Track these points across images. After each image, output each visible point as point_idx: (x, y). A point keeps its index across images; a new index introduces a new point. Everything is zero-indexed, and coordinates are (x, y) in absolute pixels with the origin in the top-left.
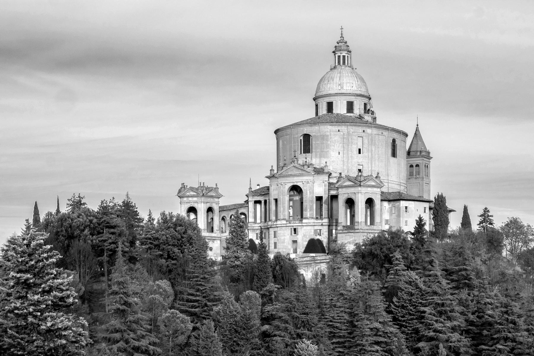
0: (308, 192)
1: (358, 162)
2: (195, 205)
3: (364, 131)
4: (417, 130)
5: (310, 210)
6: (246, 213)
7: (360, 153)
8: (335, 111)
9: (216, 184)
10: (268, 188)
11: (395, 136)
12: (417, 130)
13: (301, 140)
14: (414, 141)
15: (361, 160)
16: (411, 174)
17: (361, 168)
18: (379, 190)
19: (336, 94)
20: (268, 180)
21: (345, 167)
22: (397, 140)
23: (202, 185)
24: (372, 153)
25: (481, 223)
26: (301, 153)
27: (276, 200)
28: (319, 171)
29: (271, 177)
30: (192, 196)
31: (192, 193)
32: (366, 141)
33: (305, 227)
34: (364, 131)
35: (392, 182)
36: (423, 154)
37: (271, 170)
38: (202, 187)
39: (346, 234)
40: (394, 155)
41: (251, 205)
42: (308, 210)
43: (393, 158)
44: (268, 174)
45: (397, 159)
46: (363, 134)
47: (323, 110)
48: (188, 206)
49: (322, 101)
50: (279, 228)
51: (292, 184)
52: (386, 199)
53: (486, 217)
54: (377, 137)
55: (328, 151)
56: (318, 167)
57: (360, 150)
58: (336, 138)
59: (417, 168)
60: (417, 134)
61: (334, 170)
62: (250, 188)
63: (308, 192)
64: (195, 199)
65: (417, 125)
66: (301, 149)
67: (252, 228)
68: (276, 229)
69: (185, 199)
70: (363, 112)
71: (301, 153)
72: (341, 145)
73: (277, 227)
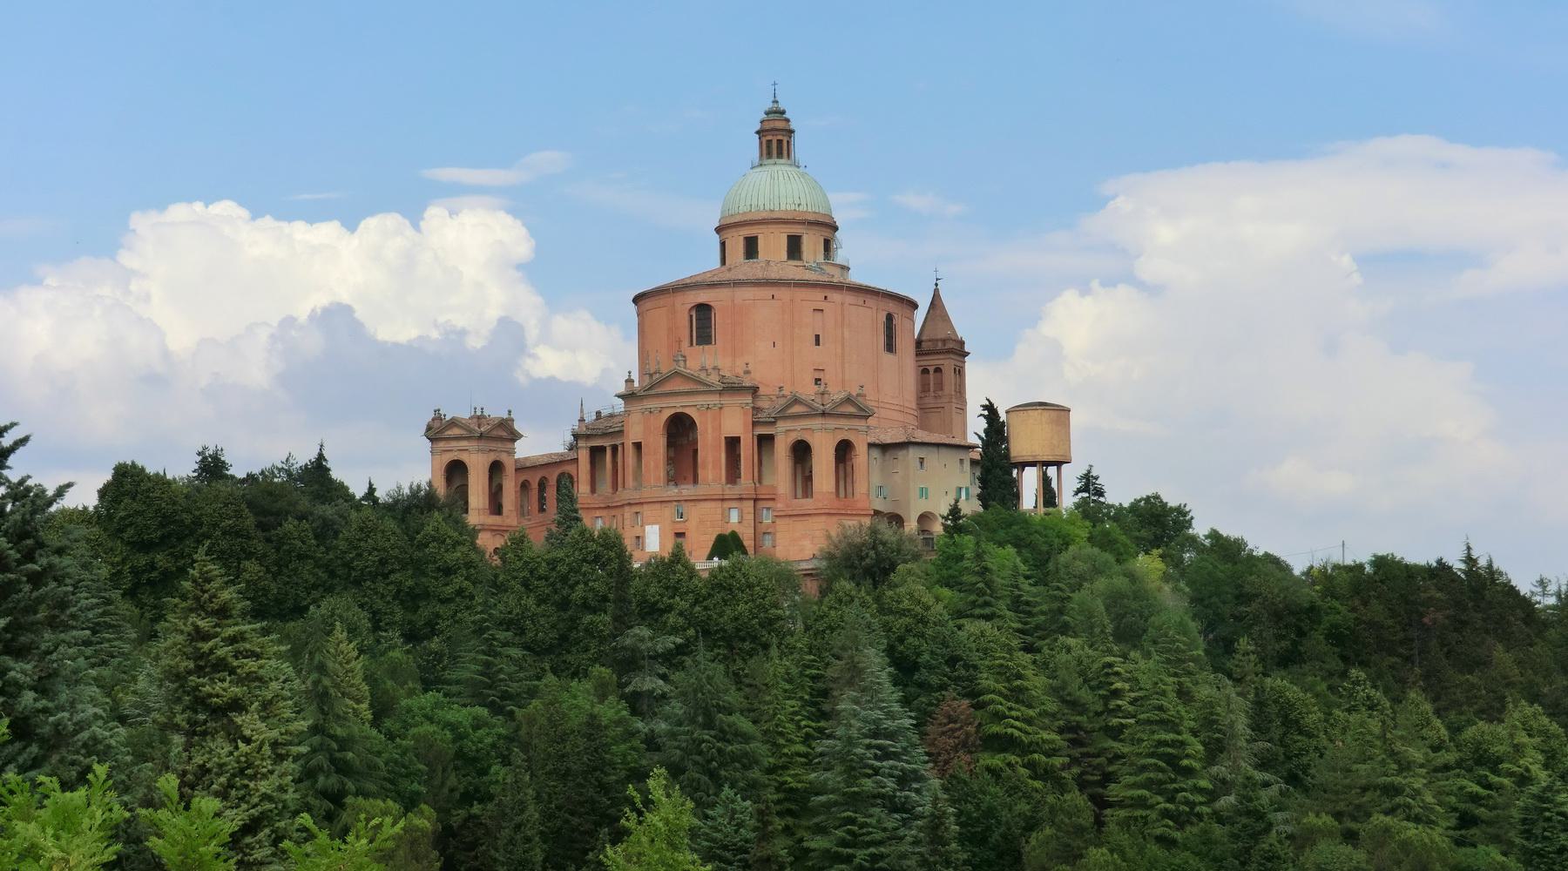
0: (709, 426)
2: (464, 457)
3: (826, 297)
6: (574, 473)
7: (818, 343)
9: (510, 412)
11: (892, 307)
13: (691, 316)
14: (929, 319)
16: (923, 389)
18: (863, 422)
20: (621, 401)
23: (479, 413)
24: (843, 345)
26: (692, 344)
27: (638, 446)
29: (628, 397)
35: (888, 406)
36: (950, 345)
37: (626, 381)
38: (479, 418)
40: (890, 347)
41: (584, 456)
42: (710, 466)
43: (890, 356)
44: (622, 389)
49: (735, 234)
50: (645, 506)
51: (673, 411)
52: (877, 442)
56: (728, 374)
57: (817, 337)
59: (938, 374)
60: (936, 303)
63: (709, 426)
64: (464, 444)
66: (691, 336)
70: (821, 259)
71: (692, 344)
73: (642, 503)
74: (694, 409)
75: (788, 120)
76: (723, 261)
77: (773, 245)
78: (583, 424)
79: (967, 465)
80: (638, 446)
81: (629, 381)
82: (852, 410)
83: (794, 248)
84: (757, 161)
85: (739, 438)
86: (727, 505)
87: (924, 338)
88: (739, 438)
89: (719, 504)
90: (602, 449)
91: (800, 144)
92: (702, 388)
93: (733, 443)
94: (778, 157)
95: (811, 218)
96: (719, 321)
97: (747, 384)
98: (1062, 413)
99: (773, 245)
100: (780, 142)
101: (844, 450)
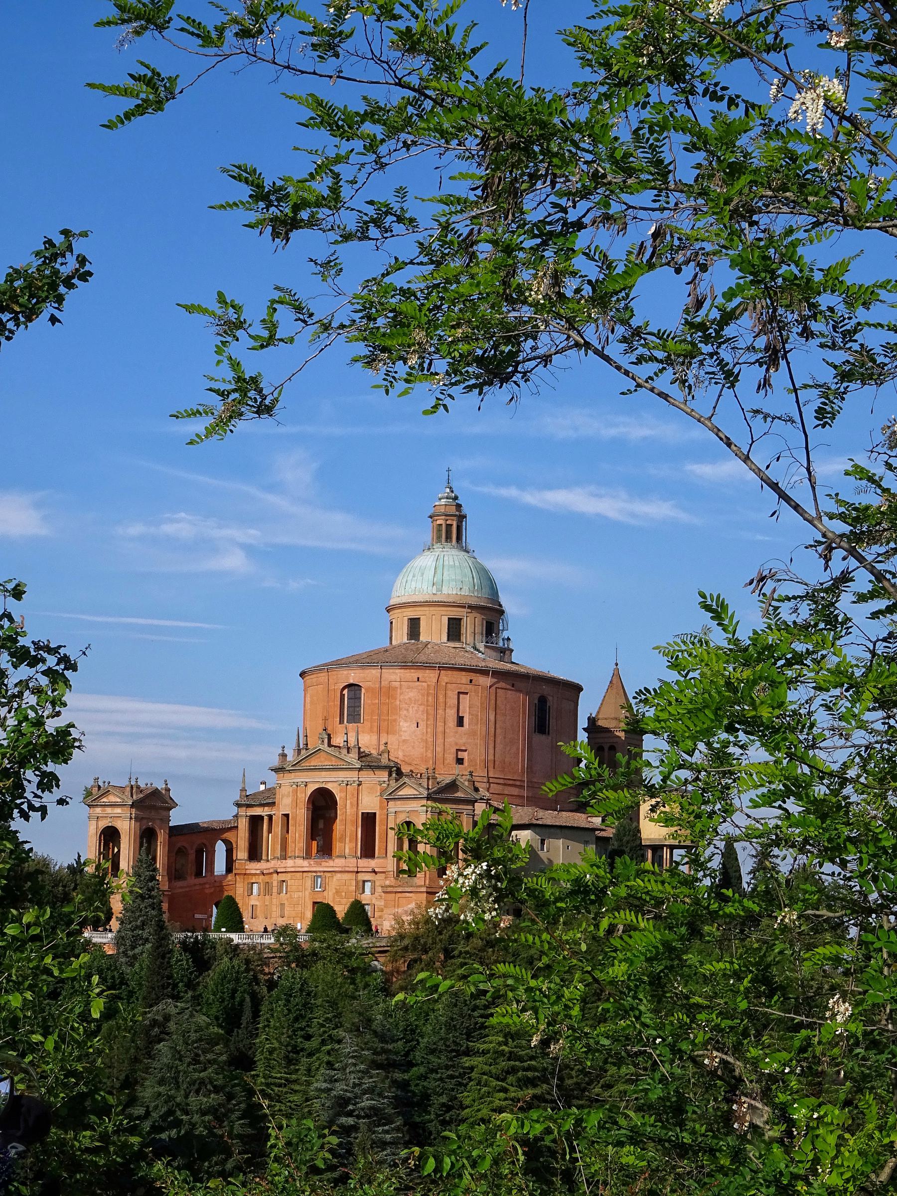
0: (348, 802)
1: (456, 744)
3: (471, 681)
4: (616, 674)
5: (350, 841)
6: (233, 841)
8: (423, 638)
9: (166, 781)
10: (271, 791)
12: (616, 674)
15: (464, 740)
19: (427, 602)
21: (429, 754)
22: (550, 698)
23: (133, 783)
25: (753, 872)
28: (368, 762)
33: (339, 875)
34: (471, 681)
39: (400, 895)
41: (243, 825)
44: (276, 762)
45: (550, 738)
46: (468, 688)
47: (401, 636)
48: (103, 824)
50: (289, 875)
51: (317, 786)
55: (395, 720)
58: (411, 694)
61: (407, 759)
62: (243, 790)
64: (118, 810)
65: (617, 664)
67: (243, 872)
68: (282, 877)
69: (98, 810)
72: (421, 708)
74: (335, 785)
76: (391, 643)
78: (244, 793)
80: (287, 816)
83: (454, 630)
84: (429, 543)
85: (375, 814)
86: (362, 877)
87: (600, 716)
88: (375, 814)
89: (353, 876)
90: (261, 818)
93: (369, 820)
94: (446, 541)
97: (384, 761)
100: (449, 527)
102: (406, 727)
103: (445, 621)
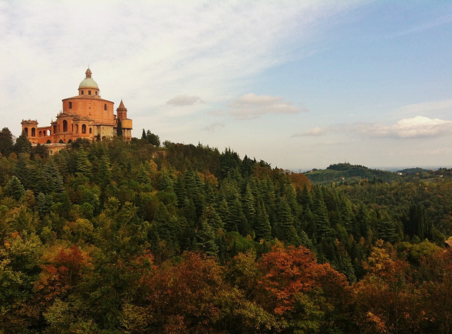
2: (27, 127)
6: (51, 130)
8: (84, 94)
11: (106, 103)
17: (90, 114)
20: (56, 119)
21: (84, 113)
27: (59, 125)
30: (26, 124)
31: (26, 123)
32: (92, 104)
33: (68, 135)
40: (105, 109)
41: (52, 127)
43: (105, 111)
44: (57, 116)
53: (149, 132)
54: (97, 103)
57: (90, 108)
60: (122, 103)
62: (52, 121)
64: (27, 125)
68: (59, 135)
75: (90, 71)
77: (86, 93)
79: (113, 128)
80: (59, 125)
81: (58, 115)
82: (85, 119)
83: (90, 93)
89: (70, 135)
91: (93, 76)
92: (67, 116)
95: (93, 88)
96: (72, 104)
98: (131, 121)
99: (86, 93)
101: (84, 126)
102: (80, 109)
103: (88, 91)
